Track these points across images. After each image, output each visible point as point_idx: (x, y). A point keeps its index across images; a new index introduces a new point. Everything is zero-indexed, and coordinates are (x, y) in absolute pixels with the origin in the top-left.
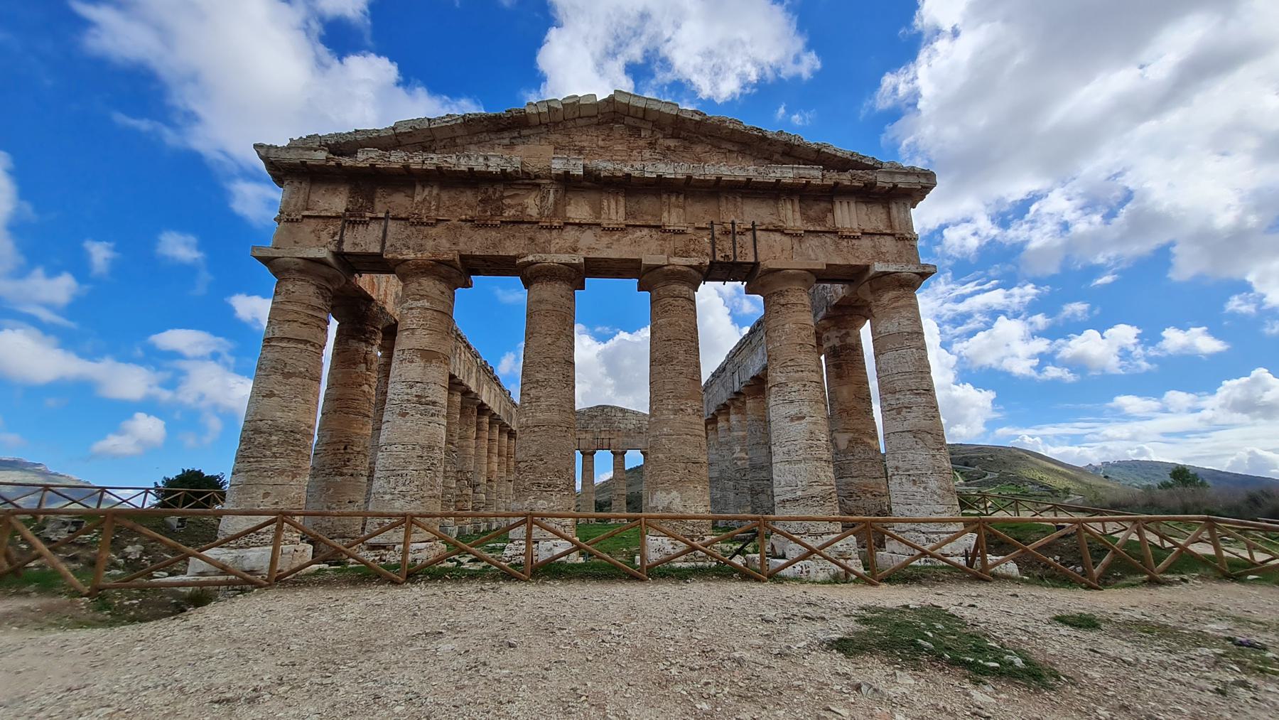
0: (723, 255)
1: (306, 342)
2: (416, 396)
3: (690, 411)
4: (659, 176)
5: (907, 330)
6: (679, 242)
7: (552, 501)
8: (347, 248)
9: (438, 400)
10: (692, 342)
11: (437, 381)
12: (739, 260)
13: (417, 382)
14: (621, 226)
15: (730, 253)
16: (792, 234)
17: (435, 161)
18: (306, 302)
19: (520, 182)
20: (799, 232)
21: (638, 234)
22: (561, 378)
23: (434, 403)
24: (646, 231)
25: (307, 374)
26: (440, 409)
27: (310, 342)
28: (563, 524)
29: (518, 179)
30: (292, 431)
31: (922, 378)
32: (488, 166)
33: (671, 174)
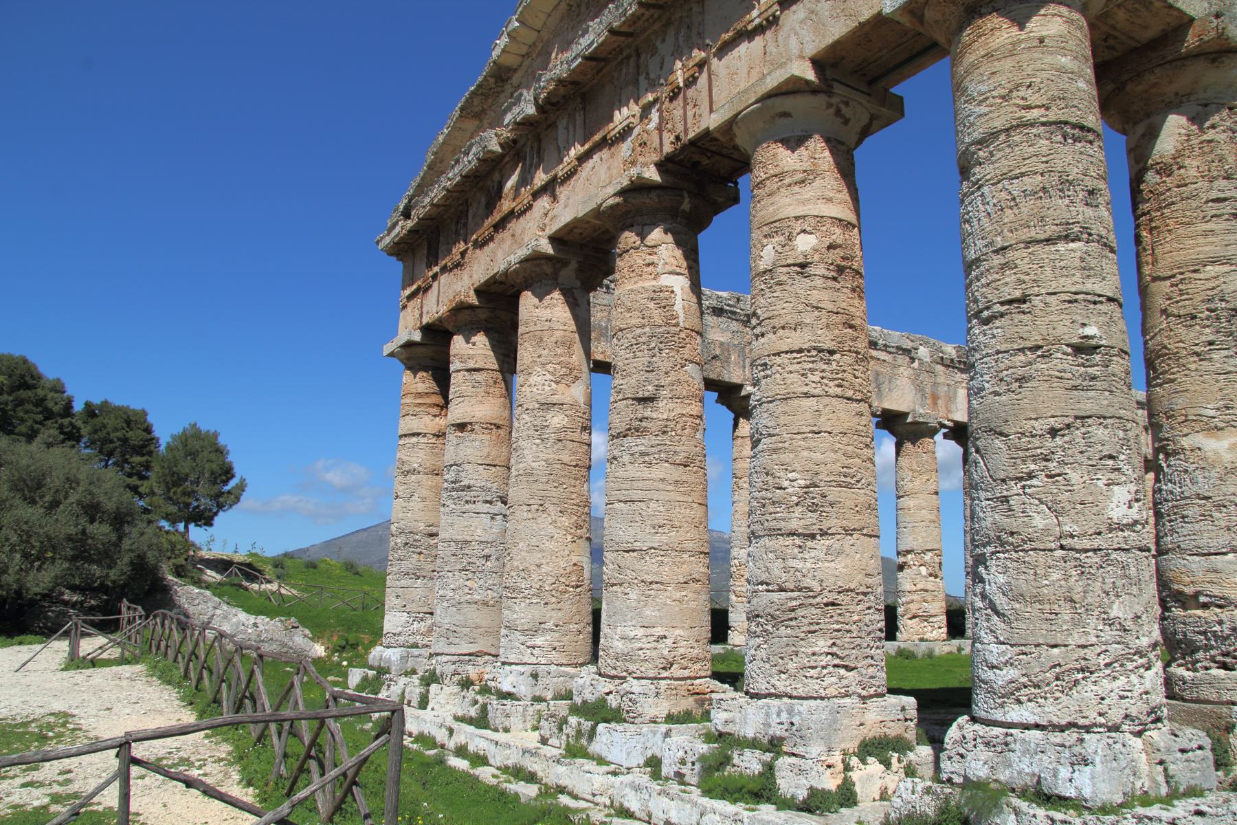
0: (672, 138)
1: (418, 434)
2: (452, 482)
3: (626, 458)
4: (586, 58)
5: (976, 136)
6: (625, 148)
7: (516, 612)
8: (425, 320)
9: (472, 482)
10: (643, 326)
11: (471, 458)
12: (691, 135)
13: (451, 466)
14: (573, 164)
15: (680, 128)
16: (761, 25)
17: (443, 184)
18: (414, 391)
19: (507, 159)
20: (770, 12)
21: (590, 164)
22: (531, 432)
23: (469, 487)
24: (596, 157)
25: (420, 469)
26: (476, 494)
27: (418, 434)
28: (529, 644)
29: (502, 156)
30: (411, 533)
31: (1004, 267)
32: (470, 162)
33: (592, 43)
